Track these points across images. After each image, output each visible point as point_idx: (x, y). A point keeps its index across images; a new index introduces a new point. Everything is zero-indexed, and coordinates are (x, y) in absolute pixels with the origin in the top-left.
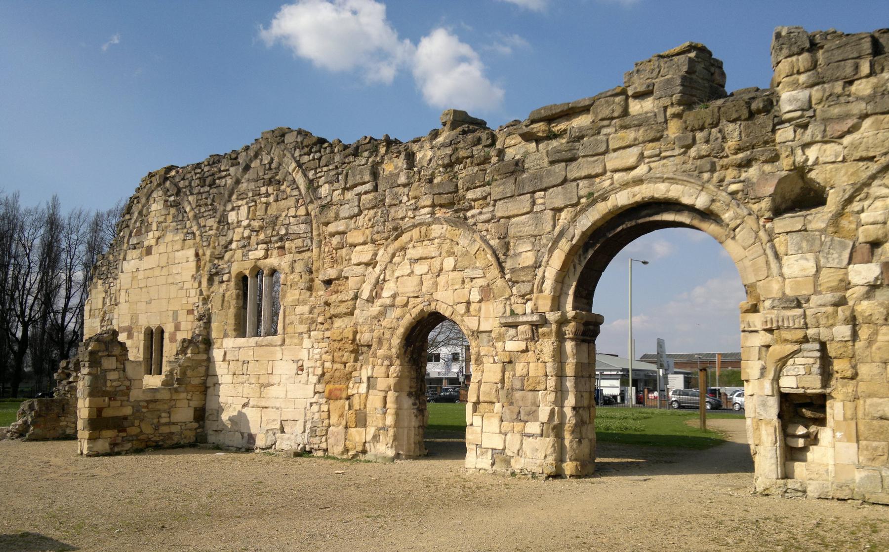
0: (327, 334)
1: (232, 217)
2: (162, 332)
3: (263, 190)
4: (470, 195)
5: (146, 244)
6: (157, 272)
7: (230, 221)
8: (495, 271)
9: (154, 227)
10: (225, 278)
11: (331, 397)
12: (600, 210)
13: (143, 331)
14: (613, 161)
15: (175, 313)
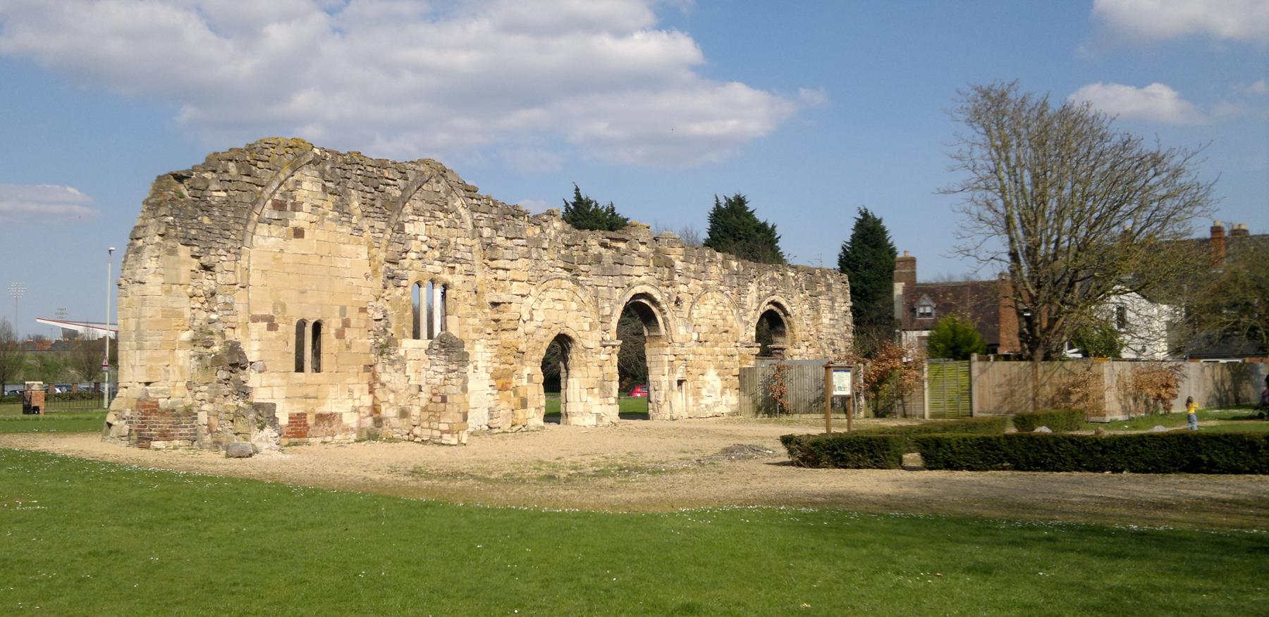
0: (495, 342)
1: (409, 228)
2: (317, 327)
3: (441, 215)
4: (582, 267)
5: (292, 224)
6: (316, 260)
7: (407, 231)
8: (595, 316)
9: (306, 207)
10: (403, 283)
11: (503, 388)
12: (633, 292)
13: (295, 323)
14: (637, 270)
15: (343, 310)
